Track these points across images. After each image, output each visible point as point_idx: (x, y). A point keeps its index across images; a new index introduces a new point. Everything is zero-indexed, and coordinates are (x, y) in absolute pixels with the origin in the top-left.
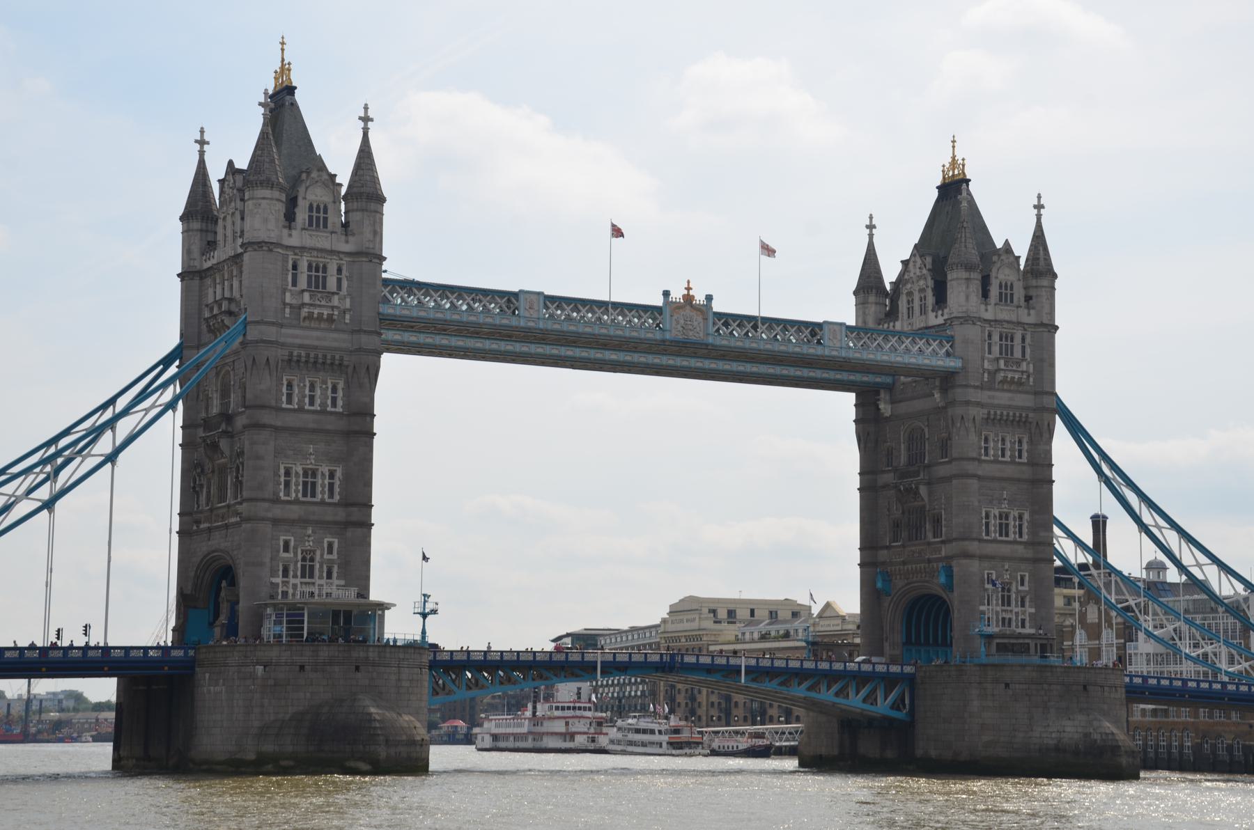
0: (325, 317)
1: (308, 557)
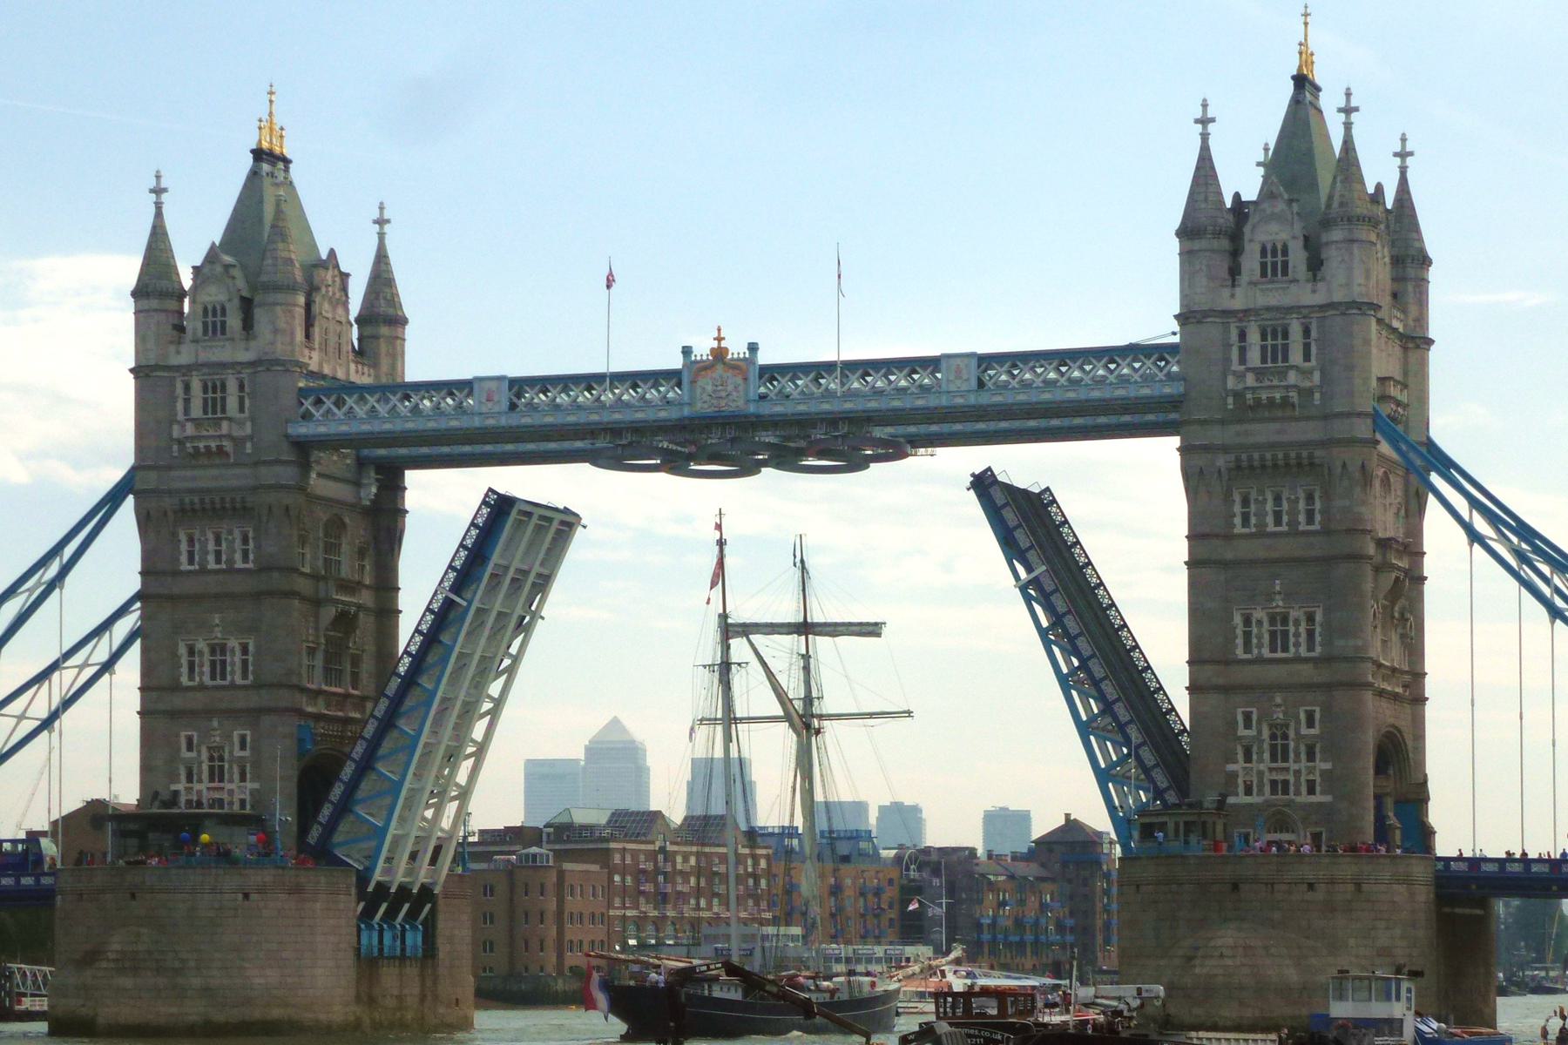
0: (214, 449)
1: (216, 755)
